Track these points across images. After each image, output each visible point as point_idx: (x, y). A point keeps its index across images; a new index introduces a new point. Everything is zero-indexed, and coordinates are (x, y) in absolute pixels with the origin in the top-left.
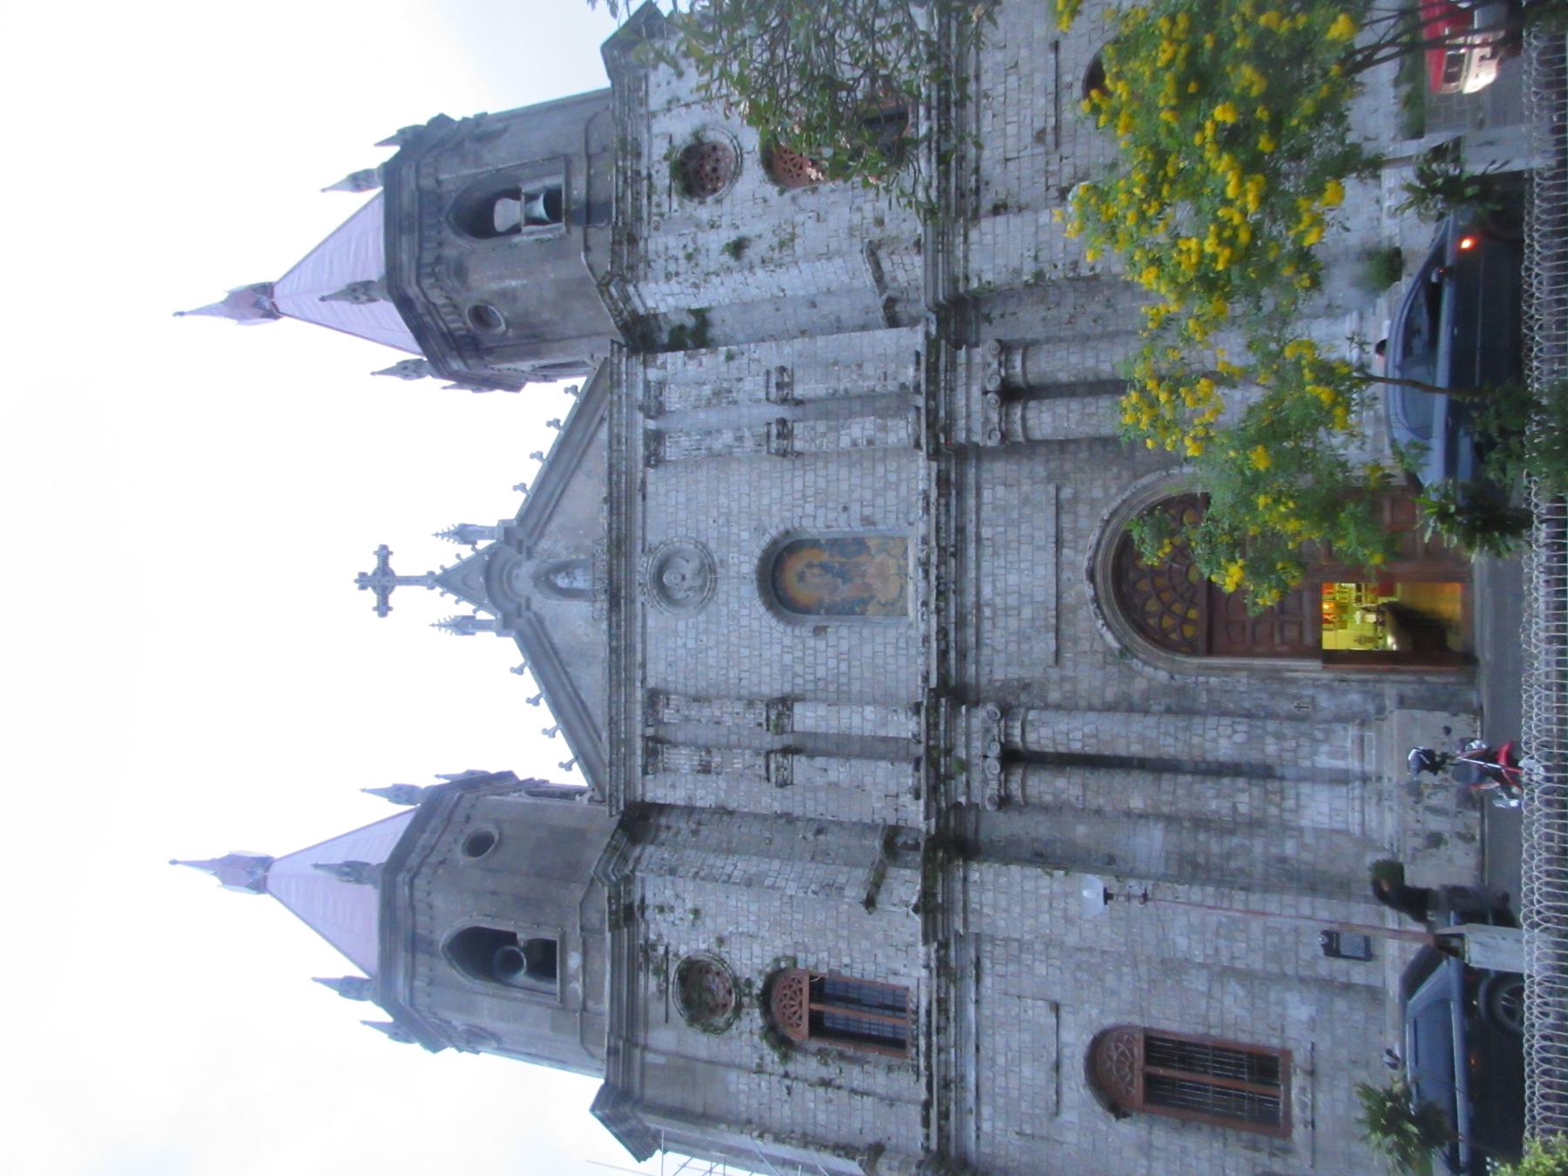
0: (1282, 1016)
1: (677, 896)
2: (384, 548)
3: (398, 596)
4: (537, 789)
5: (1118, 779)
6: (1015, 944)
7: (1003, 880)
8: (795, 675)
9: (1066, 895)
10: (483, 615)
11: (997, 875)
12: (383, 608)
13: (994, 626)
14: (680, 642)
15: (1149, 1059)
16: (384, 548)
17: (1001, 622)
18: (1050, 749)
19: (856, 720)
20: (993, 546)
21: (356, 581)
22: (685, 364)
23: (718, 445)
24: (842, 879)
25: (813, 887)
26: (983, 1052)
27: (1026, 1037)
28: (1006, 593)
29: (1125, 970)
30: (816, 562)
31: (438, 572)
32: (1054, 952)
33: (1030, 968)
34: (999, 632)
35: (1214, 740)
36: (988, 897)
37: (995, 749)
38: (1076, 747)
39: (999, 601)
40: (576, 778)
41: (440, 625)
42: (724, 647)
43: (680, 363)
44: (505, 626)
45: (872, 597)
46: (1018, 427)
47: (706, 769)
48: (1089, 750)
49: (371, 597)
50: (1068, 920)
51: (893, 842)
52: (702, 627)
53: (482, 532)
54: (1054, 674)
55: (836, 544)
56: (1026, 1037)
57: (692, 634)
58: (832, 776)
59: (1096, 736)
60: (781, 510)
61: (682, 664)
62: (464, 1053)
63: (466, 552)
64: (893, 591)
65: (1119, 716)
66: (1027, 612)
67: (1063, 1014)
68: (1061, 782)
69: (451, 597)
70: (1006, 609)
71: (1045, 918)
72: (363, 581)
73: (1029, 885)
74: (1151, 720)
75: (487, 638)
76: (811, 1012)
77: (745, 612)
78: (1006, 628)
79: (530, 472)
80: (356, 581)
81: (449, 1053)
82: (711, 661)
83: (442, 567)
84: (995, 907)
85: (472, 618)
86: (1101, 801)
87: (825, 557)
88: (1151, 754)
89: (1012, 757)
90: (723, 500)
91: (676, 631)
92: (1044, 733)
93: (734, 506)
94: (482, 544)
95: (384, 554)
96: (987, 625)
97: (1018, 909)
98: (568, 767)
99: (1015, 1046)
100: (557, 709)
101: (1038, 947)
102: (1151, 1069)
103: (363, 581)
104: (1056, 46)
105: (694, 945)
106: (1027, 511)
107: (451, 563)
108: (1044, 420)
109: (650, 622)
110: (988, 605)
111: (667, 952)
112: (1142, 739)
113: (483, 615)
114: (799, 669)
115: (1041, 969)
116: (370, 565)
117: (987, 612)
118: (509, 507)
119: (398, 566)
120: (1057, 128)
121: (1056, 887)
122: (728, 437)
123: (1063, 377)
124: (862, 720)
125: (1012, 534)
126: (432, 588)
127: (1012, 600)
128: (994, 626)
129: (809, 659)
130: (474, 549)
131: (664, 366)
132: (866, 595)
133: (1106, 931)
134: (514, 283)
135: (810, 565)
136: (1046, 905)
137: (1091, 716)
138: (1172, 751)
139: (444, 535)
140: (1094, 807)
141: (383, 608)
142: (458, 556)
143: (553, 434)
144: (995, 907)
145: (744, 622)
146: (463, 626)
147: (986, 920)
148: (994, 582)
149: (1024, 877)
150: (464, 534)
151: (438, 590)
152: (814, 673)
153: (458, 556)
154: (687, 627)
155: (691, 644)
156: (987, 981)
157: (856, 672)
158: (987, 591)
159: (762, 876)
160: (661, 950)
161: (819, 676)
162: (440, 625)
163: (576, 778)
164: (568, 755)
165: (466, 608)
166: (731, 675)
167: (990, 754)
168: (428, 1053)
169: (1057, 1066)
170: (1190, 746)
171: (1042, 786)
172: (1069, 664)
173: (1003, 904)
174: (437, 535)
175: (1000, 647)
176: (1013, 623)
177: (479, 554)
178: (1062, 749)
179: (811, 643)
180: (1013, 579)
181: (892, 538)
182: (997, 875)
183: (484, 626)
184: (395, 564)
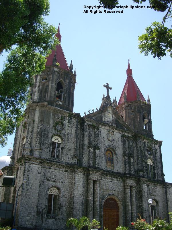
3: (105, 89)
9: (80, 187)
11: (82, 177)
12: (104, 86)
26: (55, 170)
36: (79, 176)
46: (128, 188)
49: (106, 85)
51: (80, 161)
55: (113, 159)
64: (107, 167)
66: (108, 186)
67: (61, 184)
71: (77, 183)
72: (107, 84)
73: (81, 182)
76: (56, 142)
84: (78, 177)
87: (111, 158)
89: (94, 182)
92: (97, 185)
95: (111, 89)
97: (78, 180)
102: (53, 195)
103: (107, 84)
104: (158, 196)
108: (128, 191)
109: (105, 130)
116: (110, 86)
117: (108, 180)
120: (151, 195)
121: (81, 186)
123: (132, 194)
124: (97, 161)
133: (76, 192)
135: (110, 155)
141: (104, 86)
156: (65, 173)
169: (54, 181)
171: (91, 185)
181: (113, 168)
182: (82, 177)
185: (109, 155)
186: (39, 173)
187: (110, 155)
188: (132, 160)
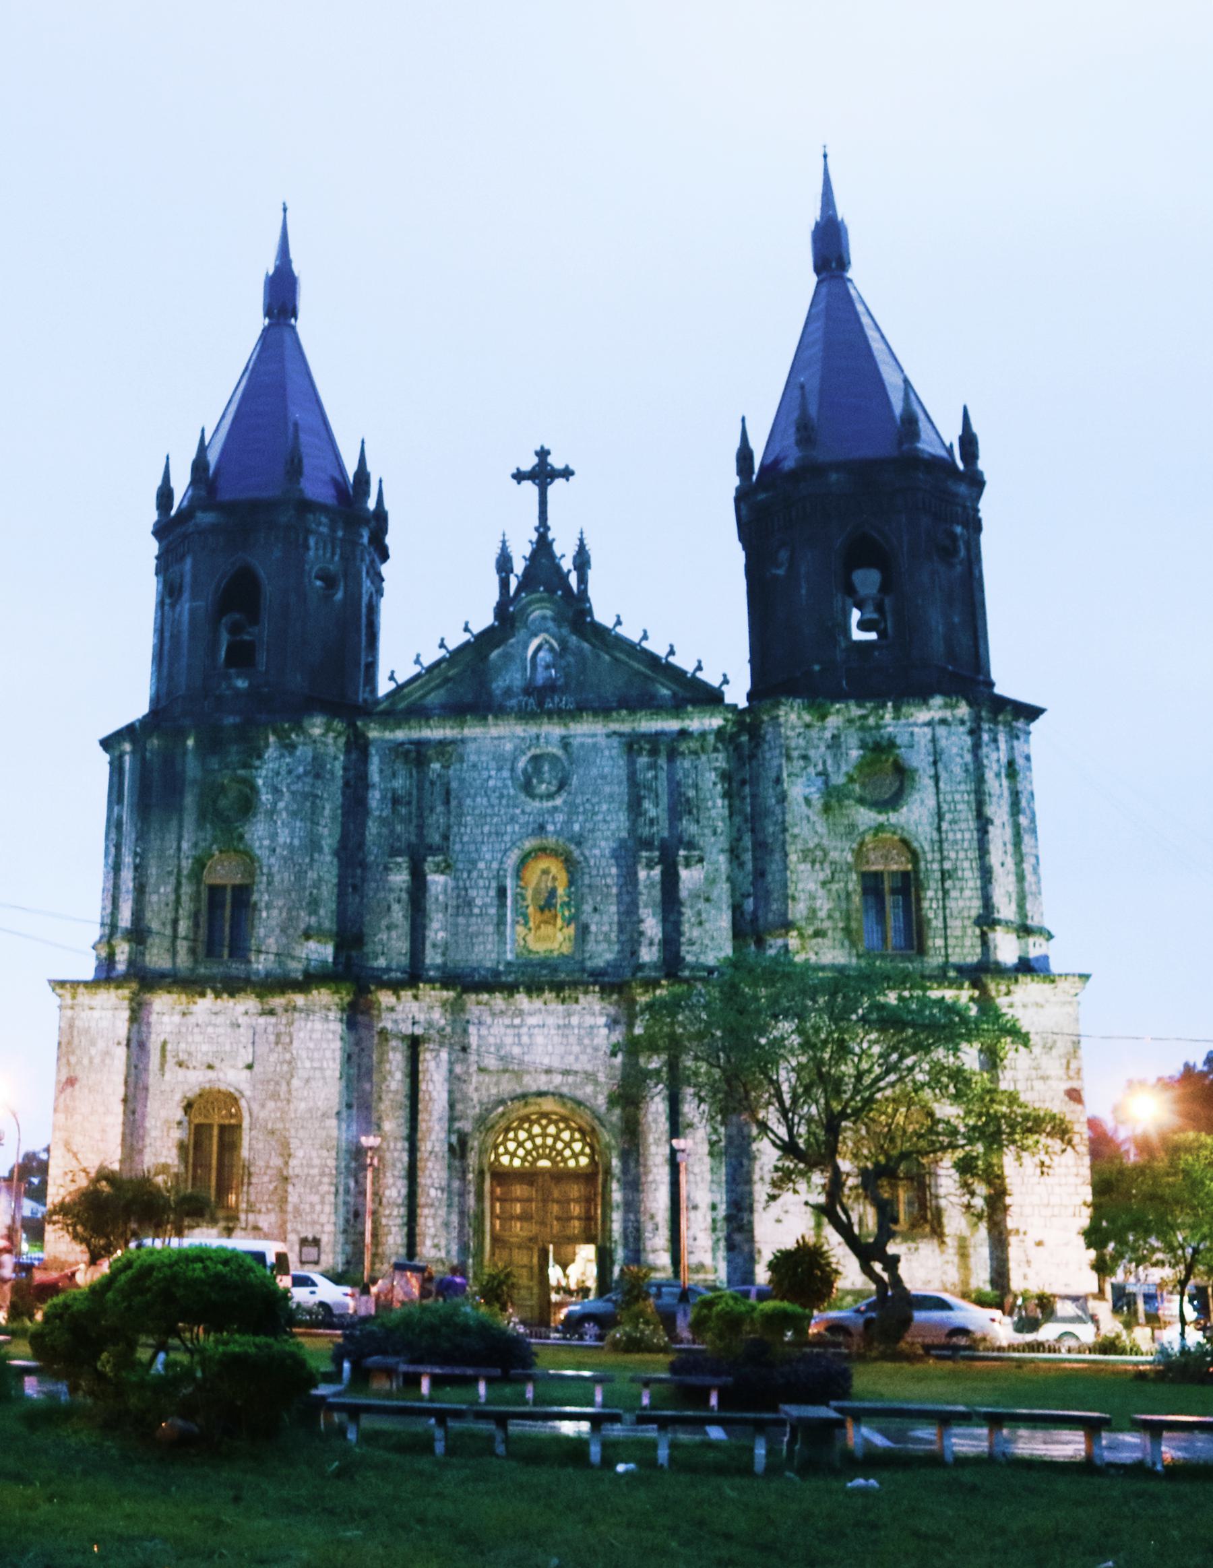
0: (260, 1212)
1: (299, 777)
2: (572, 473)
4: (372, 667)
5: (404, 1114)
6: (288, 1040)
7: (330, 1036)
8: (469, 872)
10: (514, 583)
11: (334, 1032)
12: (519, 476)
13: (507, 1027)
14: (493, 773)
15: (223, 1128)
16: (572, 473)
17: (510, 1031)
18: (421, 1068)
19: (435, 925)
20: (565, 1026)
21: (542, 448)
22: (715, 769)
23: (647, 804)
24: (322, 912)
25: (315, 891)
27: (228, 1048)
28: (531, 1036)
29: (278, 1115)
30: (557, 884)
31: (551, 535)
32: (285, 1067)
33: (271, 1051)
34: (502, 1030)
35: (431, 1176)
36: (318, 1026)
37: (418, 1031)
38: (423, 1086)
39: (524, 1030)
40: (384, 687)
41: (504, 542)
42: (489, 811)
43: (718, 764)
44: (501, 610)
45: (530, 929)
47: (396, 801)
48: (421, 1095)
50: (308, 1081)
52: (505, 792)
53: (583, 580)
54: (474, 1068)
56: (228, 1048)
57: (499, 784)
58: (396, 907)
59: (431, 1099)
60: (595, 856)
61: (476, 775)
62: (154, 562)
63: (567, 564)
65: (446, 1115)
66: (516, 1050)
68: (398, 1075)
69: (527, 550)
70: (519, 1035)
71: (308, 1064)
72: (543, 454)
73: (328, 1054)
74: (443, 1135)
75: (494, 596)
77: (517, 828)
78: (505, 1035)
79: (630, 632)
80: (542, 448)
81: (153, 547)
82: (479, 800)
83: (554, 540)
84: (312, 1031)
85: (512, 571)
86: (388, 1103)
88: (420, 1135)
89: (414, 1044)
90: (604, 807)
91: (500, 769)
93: (600, 817)
94: (573, 580)
96: (507, 1021)
97: (311, 1045)
98: (392, 678)
99: (220, 1040)
100: (437, 664)
101: (288, 1056)
103: (543, 454)
105: (263, 790)
106: (589, 1050)
107: (558, 549)
110: (522, 1020)
111: (257, 768)
112: (430, 1130)
113: (514, 583)
114: (475, 874)
115: (273, 1058)
116: (556, 462)
117: (517, 1021)
118: (603, 615)
119: (557, 488)
122: (653, 813)
124: (436, 931)
125: (573, 1039)
126: (537, 529)
127: (525, 1039)
128: (507, 1027)
129: (481, 883)
130: (569, 571)
131: (716, 750)
132: (531, 924)
133: (303, 1105)
134: (803, 592)
135: (554, 879)
136: (316, 1065)
137: (445, 1096)
138: (423, 1148)
139: (581, 540)
140: (384, 1097)
141: (519, 476)
142: (563, 556)
143: (661, 651)
144: (312, 1031)
145: (509, 829)
146: (504, 564)
147: (303, 1024)
148: (539, 1026)
149: (334, 1051)
150: (582, 561)
151: (534, 536)
152: (471, 887)
153: (563, 556)
154: (505, 779)
155: (491, 783)
157: (473, 920)
158: (532, 1021)
159: (320, 850)
160: (257, 763)
161: (470, 891)
162: (504, 542)
163: (384, 687)
164: (402, 678)
165: (519, 566)
166: (469, 818)
167: (416, 1027)
168: (151, 528)
170: (427, 1160)
172: (481, 1079)
173: (315, 1036)
174: (582, 533)
175: (492, 1031)
176: (509, 1040)
177: (564, 577)
178: (421, 1076)
179: (494, 884)
180: (540, 1040)
182: (334, 1032)
183: (504, 584)
184: (559, 482)
185: (544, 877)
186: (119, 1043)
187: (554, 879)
188: (689, 877)
